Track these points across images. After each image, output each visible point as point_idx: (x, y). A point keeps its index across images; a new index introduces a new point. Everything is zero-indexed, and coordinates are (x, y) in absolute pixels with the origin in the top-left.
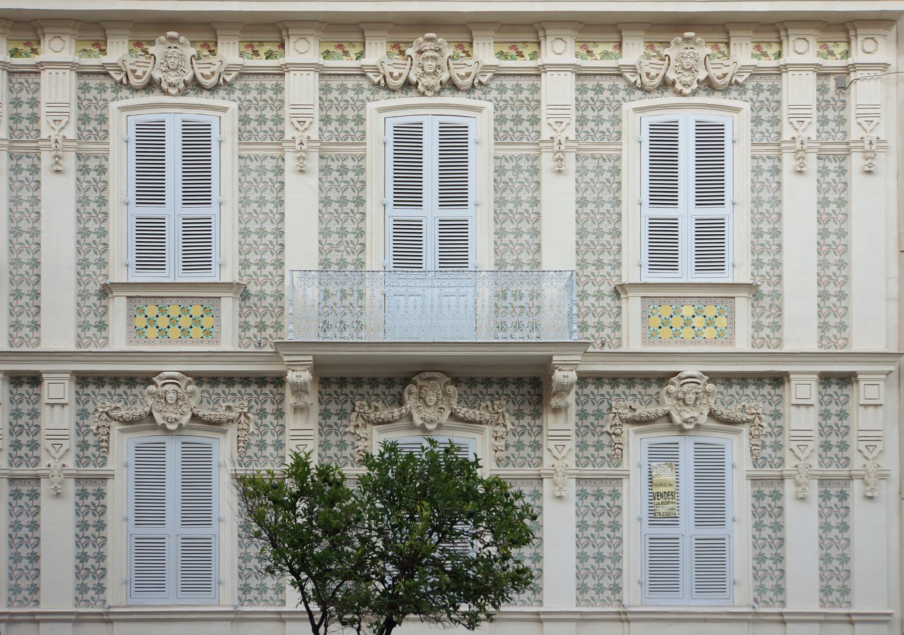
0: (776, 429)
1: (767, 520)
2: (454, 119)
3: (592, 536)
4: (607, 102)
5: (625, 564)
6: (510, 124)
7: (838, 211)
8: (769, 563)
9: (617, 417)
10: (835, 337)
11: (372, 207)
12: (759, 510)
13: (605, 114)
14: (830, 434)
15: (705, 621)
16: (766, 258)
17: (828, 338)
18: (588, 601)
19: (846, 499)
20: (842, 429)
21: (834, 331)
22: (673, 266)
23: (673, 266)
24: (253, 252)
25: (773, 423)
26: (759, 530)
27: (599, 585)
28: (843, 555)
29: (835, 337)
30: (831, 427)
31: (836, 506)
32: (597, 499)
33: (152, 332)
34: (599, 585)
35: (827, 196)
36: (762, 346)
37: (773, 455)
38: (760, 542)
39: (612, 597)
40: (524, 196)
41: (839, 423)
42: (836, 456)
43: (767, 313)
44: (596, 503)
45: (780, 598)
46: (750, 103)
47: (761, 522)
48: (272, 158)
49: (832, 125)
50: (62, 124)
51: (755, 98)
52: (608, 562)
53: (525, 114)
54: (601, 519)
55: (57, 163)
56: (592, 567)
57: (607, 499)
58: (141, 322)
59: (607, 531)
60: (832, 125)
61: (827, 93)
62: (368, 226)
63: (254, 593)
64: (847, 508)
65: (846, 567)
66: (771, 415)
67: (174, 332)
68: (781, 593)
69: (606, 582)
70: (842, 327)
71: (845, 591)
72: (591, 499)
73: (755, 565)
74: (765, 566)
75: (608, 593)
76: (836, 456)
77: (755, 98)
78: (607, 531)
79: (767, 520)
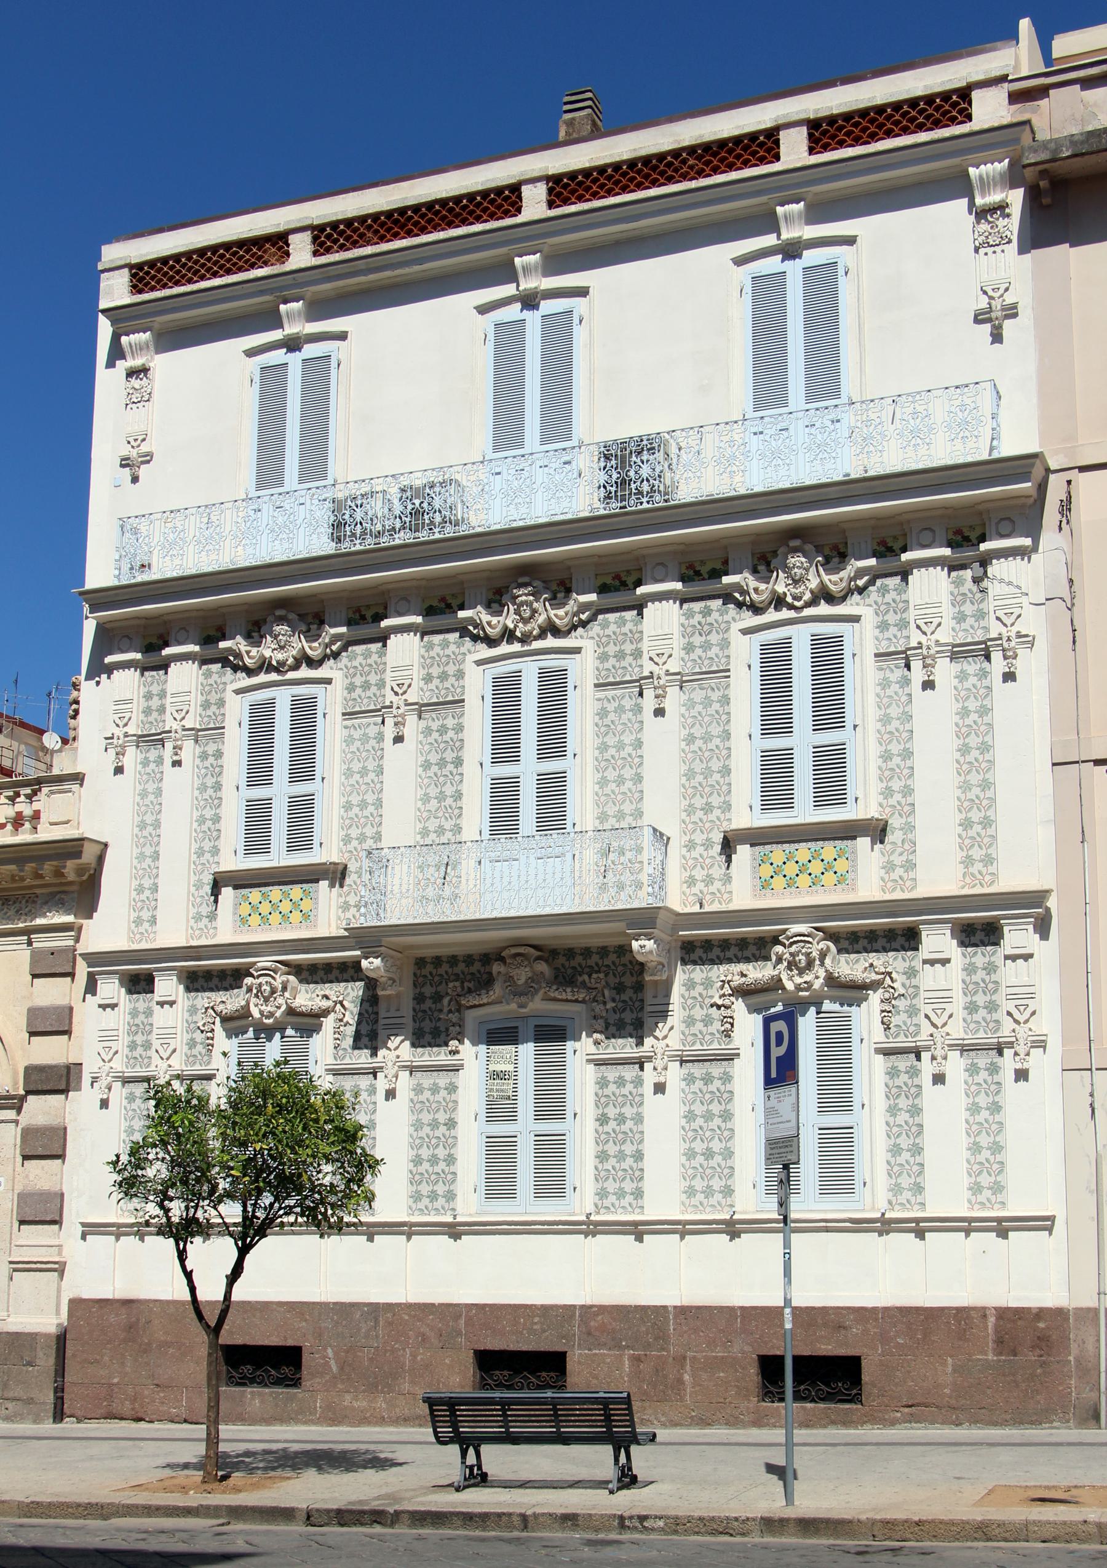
0: (911, 990)
1: (903, 1103)
2: (553, 662)
3: (701, 1128)
4: (716, 625)
5: (738, 1162)
6: (612, 661)
7: (979, 721)
8: (906, 1155)
9: (726, 985)
10: (980, 872)
11: (470, 768)
12: (894, 1091)
13: (714, 638)
14: (976, 993)
15: (827, 1230)
16: (896, 785)
17: (973, 875)
18: (696, 1206)
19: (997, 1072)
20: (990, 986)
21: (978, 866)
22: (787, 804)
23: (787, 804)
24: (354, 826)
25: (907, 983)
26: (894, 1115)
27: (708, 1187)
28: (995, 1143)
29: (980, 872)
30: (977, 983)
31: (985, 1081)
32: (706, 1084)
33: (255, 919)
34: (708, 1187)
35: (966, 704)
36: (894, 889)
37: (909, 1022)
38: (895, 1129)
39: (723, 1202)
40: (628, 739)
41: (987, 978)
42: (984, 1019)
43: (899, 850)
44: (704, 1089)
45: (919, 1199)
46: (875, 607)
47: (897, 1104)
48: (375, 724)
49: (970, 621)
50: (126, 720)
51: (880, 600)
52: (718, 1159)
53: (628, 648)
54: (710, 1107)
55: (176, 754)
56: (701, 1165)
57: (717, 1083)
58: (245, 909)
59: (717, 1121)
60: (970, 621)
61: (963, 585)
62: (465, 788)
63: (612, 1198)
64: (999, 1083)
65: (999, 1158)
66: (905, 973)
67: (275, 918)
68: (920, 1193)
69: (717, 1184)
70: (988, 860)
71: (998, 1188)
72: (699, 1084)
73: (890, 1159)
74: (901, 1160)
75: (718, 1197)
76: (984, 1019)
77: (880, 600)
78: (717, 1121)
79: (903, 1103)
